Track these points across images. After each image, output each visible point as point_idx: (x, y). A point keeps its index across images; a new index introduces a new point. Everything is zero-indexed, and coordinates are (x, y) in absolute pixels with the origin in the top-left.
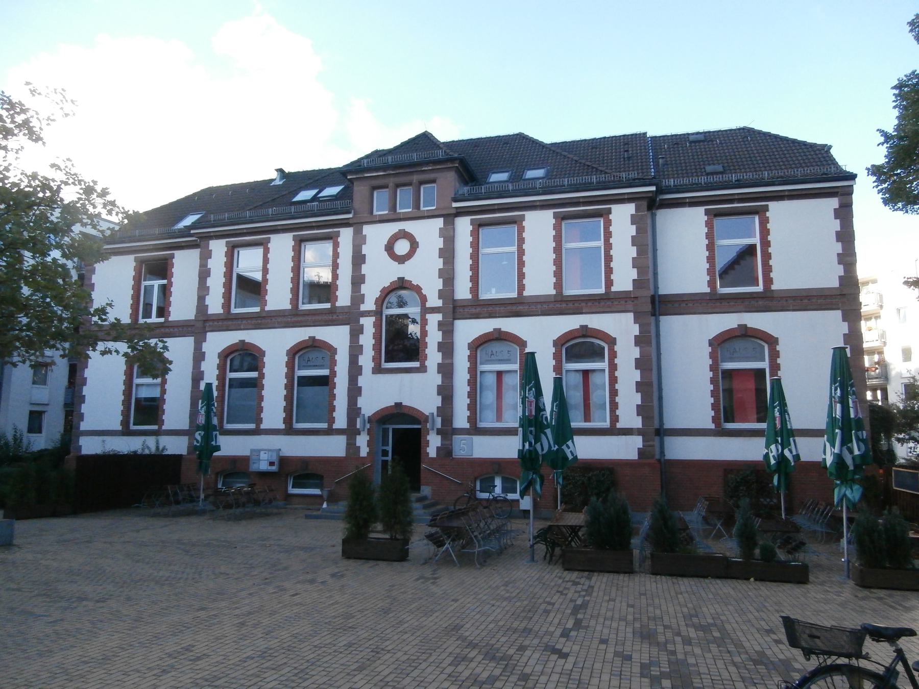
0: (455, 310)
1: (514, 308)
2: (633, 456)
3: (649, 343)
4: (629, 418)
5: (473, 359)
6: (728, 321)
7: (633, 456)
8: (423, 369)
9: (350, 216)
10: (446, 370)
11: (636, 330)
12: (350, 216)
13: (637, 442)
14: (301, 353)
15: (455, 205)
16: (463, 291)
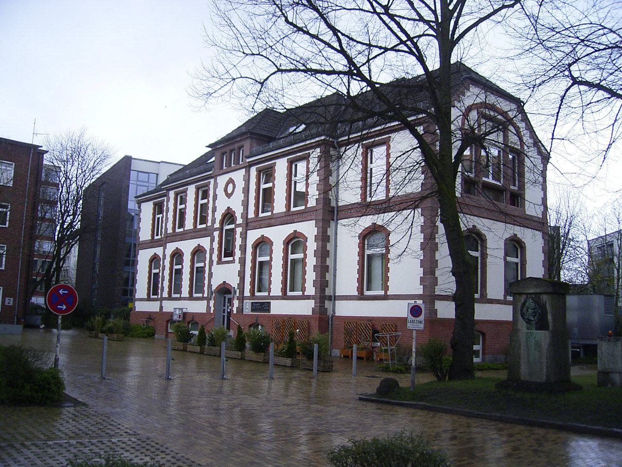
0: (248, 225)
1: (268, 221)
2: (309, 313)
3: (323, 238)
4: (310, 290)
5: (254, 255)
6: (366, 222)
7: (309, 313)
8: (233, 262)
9: (211, 172)
10: (243, 262)
11: (315, 231)
12: (211, 172)
13: (311, 303)
14: (197, 253)
15: (248, 160)
16: (251, 215)
